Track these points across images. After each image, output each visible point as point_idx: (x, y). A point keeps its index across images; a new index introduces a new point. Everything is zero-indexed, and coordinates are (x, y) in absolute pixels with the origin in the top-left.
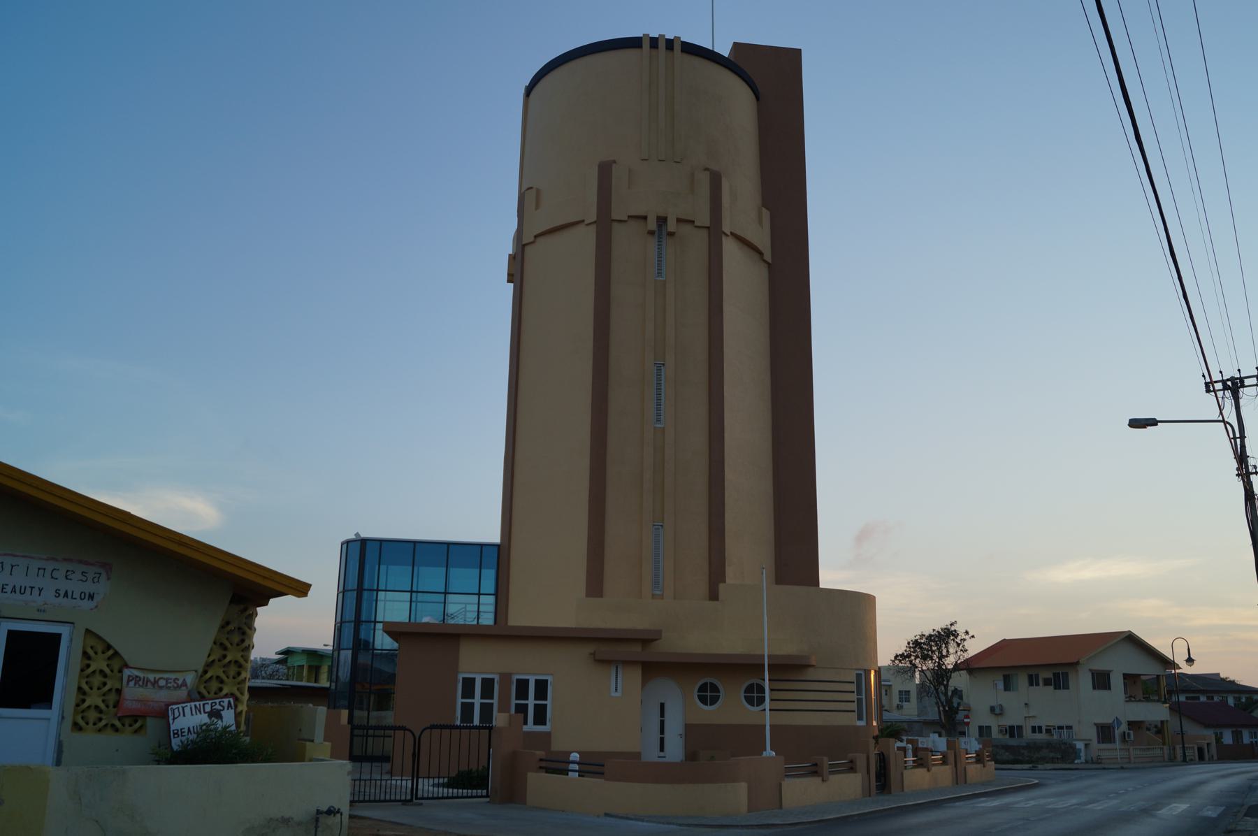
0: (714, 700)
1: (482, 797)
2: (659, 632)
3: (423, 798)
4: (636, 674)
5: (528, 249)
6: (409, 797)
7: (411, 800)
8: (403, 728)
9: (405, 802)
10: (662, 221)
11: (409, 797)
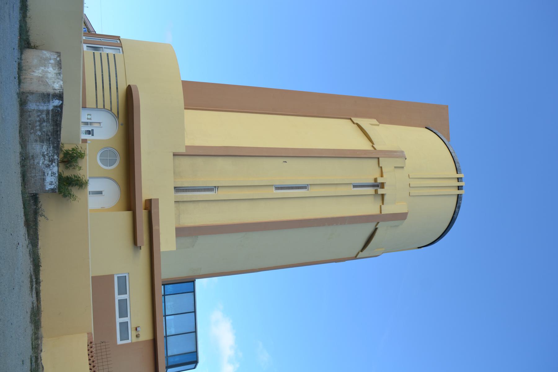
10: (382, 185)
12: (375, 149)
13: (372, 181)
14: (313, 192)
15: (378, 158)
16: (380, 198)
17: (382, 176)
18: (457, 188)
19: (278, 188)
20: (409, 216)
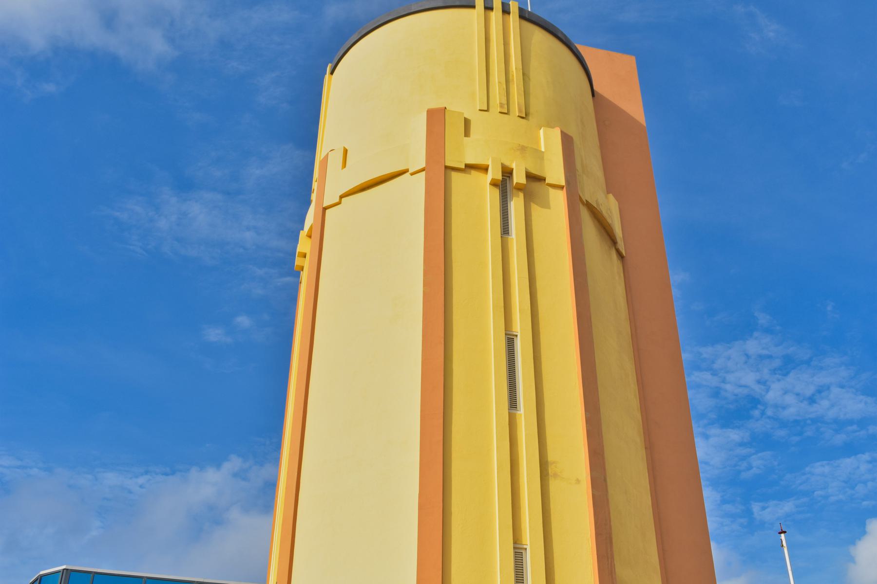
5: (327, 211)
10: (507, 173)
13: (497, 192)
14: (521, 326)
15: (446, 167)
16: (536, 186)
17: (485, 169)
18: (507, 16)
20: (565, 131)
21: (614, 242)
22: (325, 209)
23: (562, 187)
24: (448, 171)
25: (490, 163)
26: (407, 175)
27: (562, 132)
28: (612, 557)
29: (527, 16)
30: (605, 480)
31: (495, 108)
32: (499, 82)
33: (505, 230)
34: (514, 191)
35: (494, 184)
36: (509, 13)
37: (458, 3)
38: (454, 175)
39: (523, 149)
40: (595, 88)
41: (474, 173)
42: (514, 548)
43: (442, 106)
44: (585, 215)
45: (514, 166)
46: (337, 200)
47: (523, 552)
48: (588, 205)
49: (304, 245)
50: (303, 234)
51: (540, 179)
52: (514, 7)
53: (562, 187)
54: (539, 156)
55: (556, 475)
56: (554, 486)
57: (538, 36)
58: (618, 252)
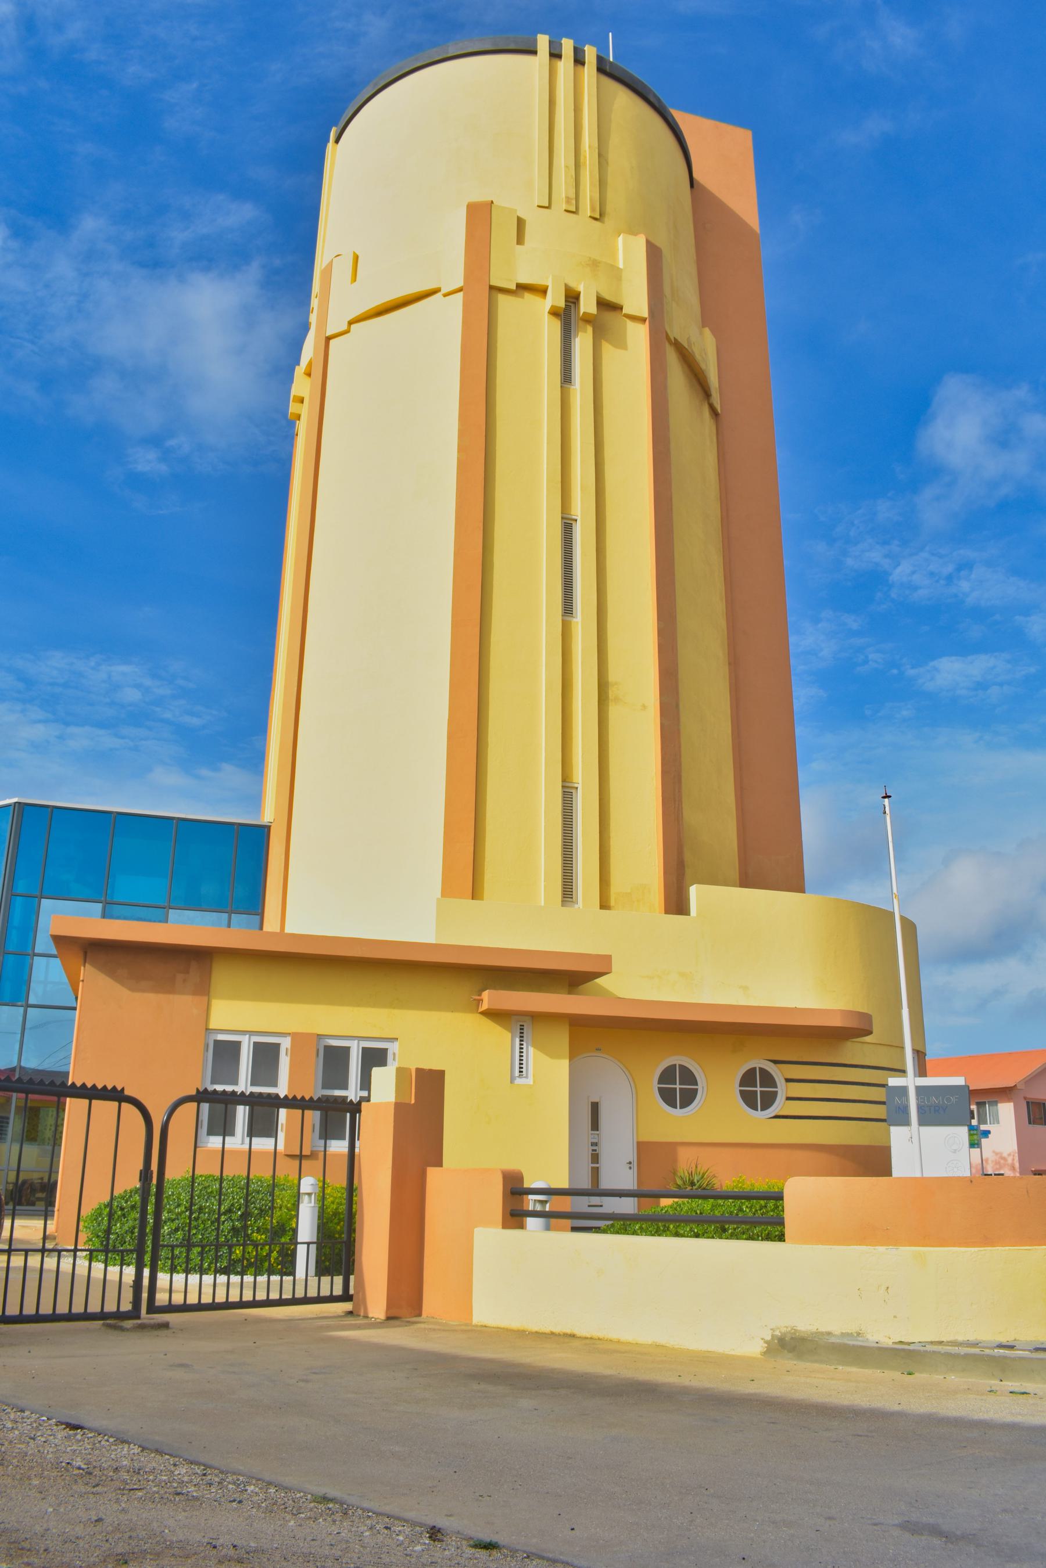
0: (688, 1098)
1: (332, 1299)
2: (608, 959)
3: (171, 1308)
4: (562, 1038)
5: (332, 342)
6: (126, 1306)
7: (134, 1313)
8: (116, 1095)
9: (112, 1320)
10: (572, 298)
11: (126, 1306)
12: (460, 290)
13: (557, 325)
14: (582, 508)
15: (492, 288)
16: (609, 316)
17: (543, 291)
18: (580, 67)
19: (568, 608)
20: (651, 239)
21: (707, 394)
22: (328, 339)
23: (643, 320)
24: (494, 292)
25: (549, 282)
26: (439, 295)
27: (648, 242)
28: (680, 801)
29: (608, 69)
30: (677, 706)
31: (560, 203)
32: (566, 167)
33: (567, 377)
34: (581, 323)
35: (554, 313)
36: (583, 64)
37: (512, 47)
38: (502, 298)
39: (594, 264)
40: (695, 175)
41: (528, 296)
42: (563, 787)
43: (490, 199)
44: (672, 358)
45: (581, 288)
46: (345, 327)
47: (573, 791)
48: (677, 345)
49: (301, 386)
50: (300, 371)
51: (616, 308)
52: (590, 53)
53: (643, 320)
54: (616, 274)
55: (617, 700)
56: (614, 711)
57: (623, 99)
58: (712, 408)
